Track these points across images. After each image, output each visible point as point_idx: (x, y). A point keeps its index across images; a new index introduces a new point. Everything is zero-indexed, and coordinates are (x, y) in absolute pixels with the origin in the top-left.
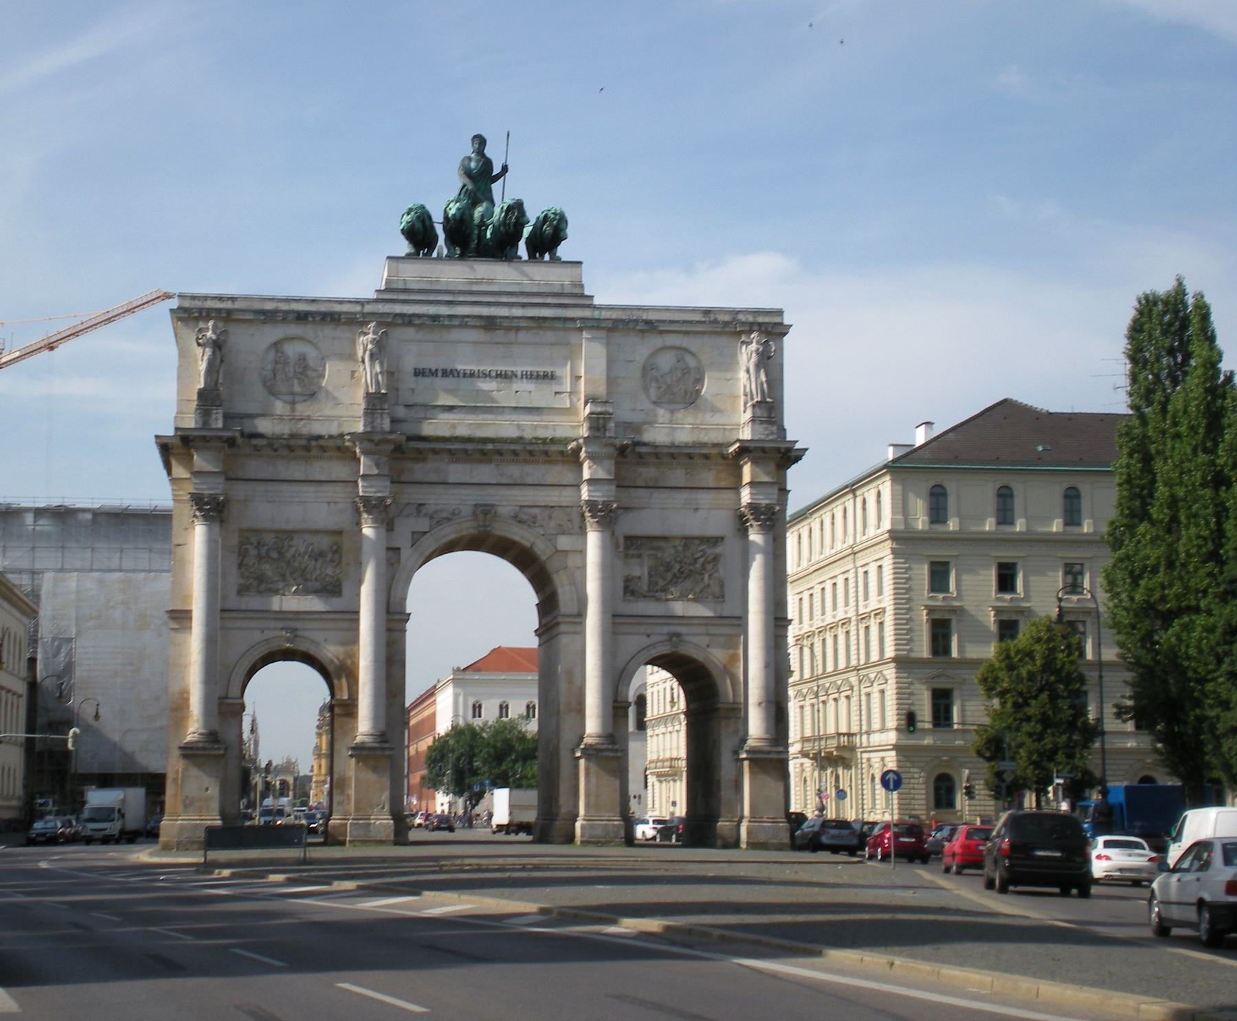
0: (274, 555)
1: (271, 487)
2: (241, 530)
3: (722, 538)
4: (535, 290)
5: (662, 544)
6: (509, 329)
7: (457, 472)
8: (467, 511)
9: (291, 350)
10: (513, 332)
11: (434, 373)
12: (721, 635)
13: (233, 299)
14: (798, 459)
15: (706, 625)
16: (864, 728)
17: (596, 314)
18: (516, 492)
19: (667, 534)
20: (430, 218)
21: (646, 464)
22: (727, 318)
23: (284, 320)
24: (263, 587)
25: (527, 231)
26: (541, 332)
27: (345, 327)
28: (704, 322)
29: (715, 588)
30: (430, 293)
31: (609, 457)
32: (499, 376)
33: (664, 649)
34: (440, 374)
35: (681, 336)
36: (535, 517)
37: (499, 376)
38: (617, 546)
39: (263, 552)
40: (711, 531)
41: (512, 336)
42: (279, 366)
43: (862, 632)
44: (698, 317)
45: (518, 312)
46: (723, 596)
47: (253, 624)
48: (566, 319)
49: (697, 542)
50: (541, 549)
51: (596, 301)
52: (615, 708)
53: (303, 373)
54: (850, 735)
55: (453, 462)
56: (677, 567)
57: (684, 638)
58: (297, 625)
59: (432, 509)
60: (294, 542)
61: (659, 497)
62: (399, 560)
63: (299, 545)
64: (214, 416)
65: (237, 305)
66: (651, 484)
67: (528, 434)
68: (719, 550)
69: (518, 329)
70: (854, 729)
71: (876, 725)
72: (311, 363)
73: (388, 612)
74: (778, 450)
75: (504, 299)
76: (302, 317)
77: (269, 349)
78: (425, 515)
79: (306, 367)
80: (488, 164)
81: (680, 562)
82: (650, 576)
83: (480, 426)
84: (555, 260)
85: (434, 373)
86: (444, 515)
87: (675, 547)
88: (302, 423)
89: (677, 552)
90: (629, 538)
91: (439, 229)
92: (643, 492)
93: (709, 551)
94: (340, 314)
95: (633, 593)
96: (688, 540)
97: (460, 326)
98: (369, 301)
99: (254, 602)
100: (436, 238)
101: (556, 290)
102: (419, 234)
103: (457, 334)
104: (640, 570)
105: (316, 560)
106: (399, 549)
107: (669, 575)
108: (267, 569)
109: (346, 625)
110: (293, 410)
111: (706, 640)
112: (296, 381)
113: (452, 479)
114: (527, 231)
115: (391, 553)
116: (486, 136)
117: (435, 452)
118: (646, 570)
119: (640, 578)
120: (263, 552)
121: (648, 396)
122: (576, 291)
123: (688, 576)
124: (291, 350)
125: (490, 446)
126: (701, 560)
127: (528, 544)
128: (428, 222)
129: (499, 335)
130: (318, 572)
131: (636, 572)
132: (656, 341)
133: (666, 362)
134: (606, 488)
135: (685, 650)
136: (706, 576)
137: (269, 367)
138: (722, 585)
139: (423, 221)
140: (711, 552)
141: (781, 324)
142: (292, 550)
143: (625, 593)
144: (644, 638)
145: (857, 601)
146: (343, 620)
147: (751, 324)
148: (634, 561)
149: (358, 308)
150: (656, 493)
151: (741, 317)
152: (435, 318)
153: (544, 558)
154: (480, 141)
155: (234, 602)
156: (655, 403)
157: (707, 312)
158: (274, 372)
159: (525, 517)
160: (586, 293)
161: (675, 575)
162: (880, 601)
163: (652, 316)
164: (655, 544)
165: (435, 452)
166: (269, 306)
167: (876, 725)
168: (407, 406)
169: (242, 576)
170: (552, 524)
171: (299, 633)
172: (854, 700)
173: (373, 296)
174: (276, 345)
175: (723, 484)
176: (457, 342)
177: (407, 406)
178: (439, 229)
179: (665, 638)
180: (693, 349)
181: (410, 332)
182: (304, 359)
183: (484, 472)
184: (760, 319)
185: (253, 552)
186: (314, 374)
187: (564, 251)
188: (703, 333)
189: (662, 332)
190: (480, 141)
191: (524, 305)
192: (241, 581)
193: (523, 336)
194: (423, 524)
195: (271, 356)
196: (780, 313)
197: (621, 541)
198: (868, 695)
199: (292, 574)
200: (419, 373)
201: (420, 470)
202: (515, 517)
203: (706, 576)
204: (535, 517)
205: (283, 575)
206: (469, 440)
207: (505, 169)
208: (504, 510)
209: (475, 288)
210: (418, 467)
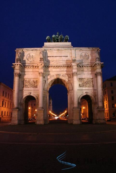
0: (28, 82)
5: (84, 79)
9: (31, 55)
18: (62, 72)
32: (60, 57)
37: (60, 57)
52: (78, 103)
53: (33, 57)
56: (87, 82)
68: (93, 80)
83: (57, 63)
107: (86, 84)
108: (27, 84)
110: (31, 62)
118: (82, 83)
131: (81, 83)
133: (83, 54)
152: (51, 49)
175: (93, 70)
180: (87, 53)
183: (58, 70)
189: (83, 50)
197: (78, 79)
208: (61, 75)
209: (56, 46)
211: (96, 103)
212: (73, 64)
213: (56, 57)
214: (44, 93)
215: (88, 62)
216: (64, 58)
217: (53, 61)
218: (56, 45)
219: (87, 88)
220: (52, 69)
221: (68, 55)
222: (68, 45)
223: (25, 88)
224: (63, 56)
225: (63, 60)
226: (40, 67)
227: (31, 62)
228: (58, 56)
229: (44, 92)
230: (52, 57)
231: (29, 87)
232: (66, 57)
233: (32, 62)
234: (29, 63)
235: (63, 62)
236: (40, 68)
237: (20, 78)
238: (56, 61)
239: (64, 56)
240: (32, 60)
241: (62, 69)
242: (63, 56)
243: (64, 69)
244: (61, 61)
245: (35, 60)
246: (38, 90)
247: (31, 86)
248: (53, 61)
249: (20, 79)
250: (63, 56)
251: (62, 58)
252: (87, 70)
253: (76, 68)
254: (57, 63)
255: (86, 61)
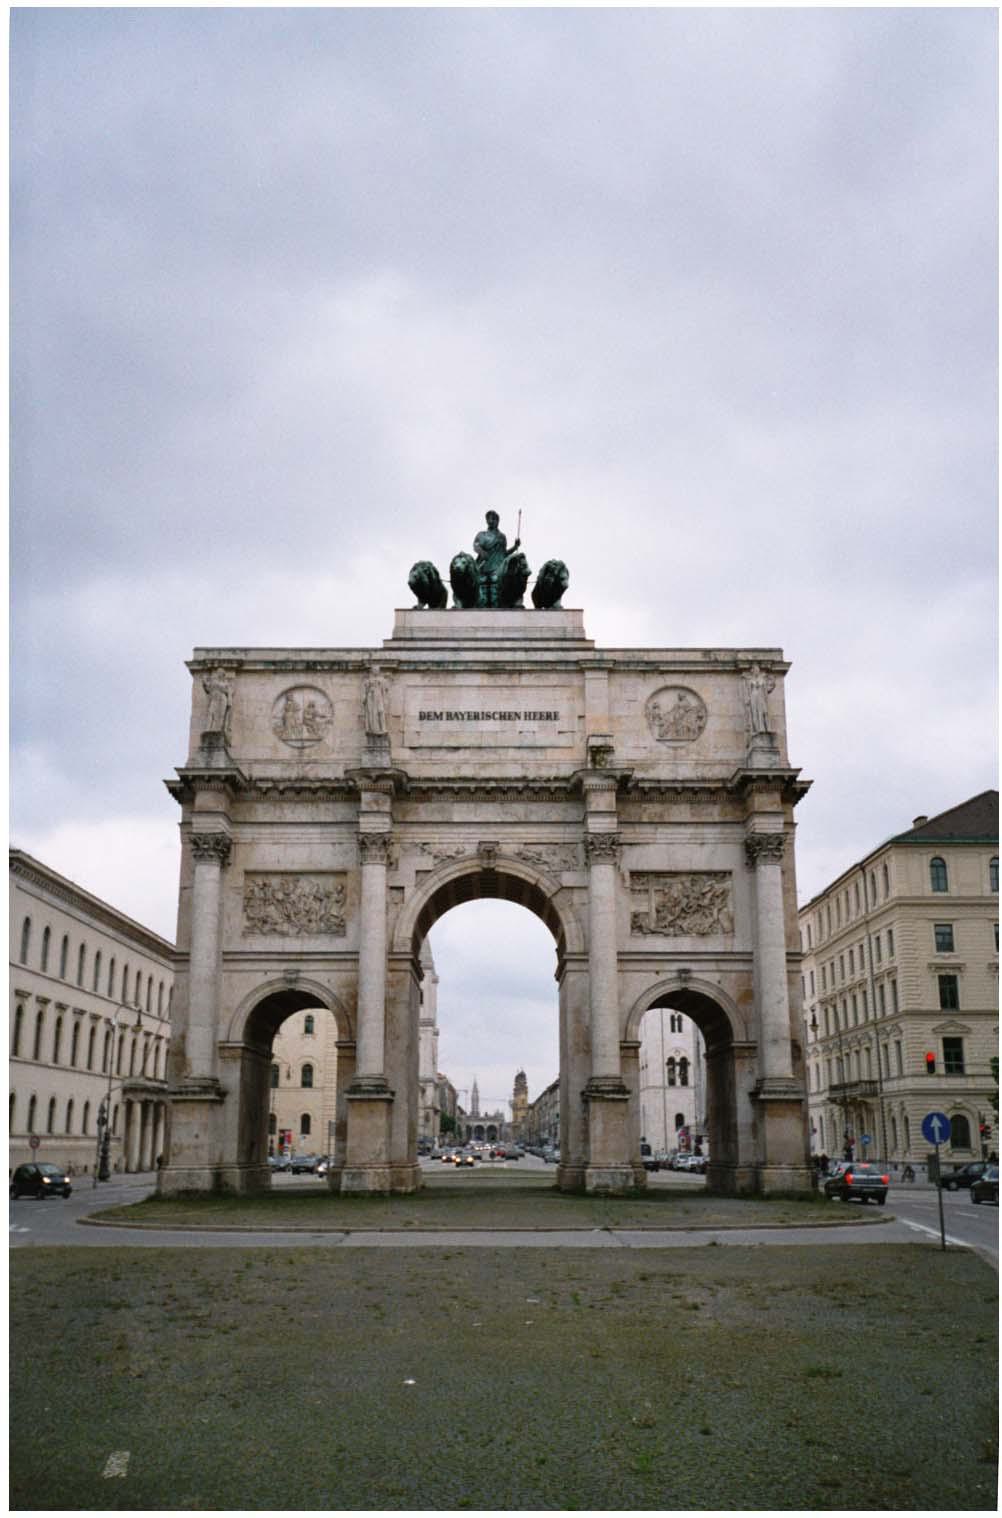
1: (275, 830)
2: (248, 873)
3: (730, 873)
4: (538, 635)
5: (668, 880)
6: (511, 672)
7: (461, 812)
8: (471, 850)
10: (516, 676)
11: (438, 717)
12: (731, 971)
13: (246, 650)
14: (804, 791)
15: (717, 961)
16: (884, 1076)
17: (598, 656)
18: (519, 829)
19: (673, 869)
20: (437, 573)
21: (651, 801)
22: (728, 657)
23: (294, 671)
24: (267, 928)
25: (531, 586)
26: (544, 675)
27: (352, 675)
28: (708, 662)
29: (726, 924)
30: (434, 640)
31: (609, 790)
32: (504, 717)
33: (674, 987)
34: (444, 716)
35: (682, 675)
36: (540, 854)
37: (504, 717)
38: (623, 880)
39: (269, 894)
40: (717, 866)
41: (515, 680)
42: (290, 713)
43: (877, 991)
44: (698, 657)
45: (520, 656)
46: (733, 931)
47: (257, 966)
48: (567, 662)
49: (705, 877)
50: (547, 886)
51: (597, 645)
54: (872, 1082)
55: (457, 802)
56: (685, 901)
57: (695, 975)
58: (302, 966)
59: (435, 849)
60: (300, 884)
61: (663, 833)
62: (403, 900)
63: (306, 886)
64: (215, 758)
65: (252, 656)
66: (656, 820)
67: (531, 775)
68: (727, 884)
69: (521, 672)
70: (876, 1077)
71: (894, 1073)
72: (320, 711)
73: (390, 952)
74: (781, 778)
75: (508, 644)
76: (311, 667)
77: (279, 698)
78: (430, 853)
79: (315, 715)
80: (502, 540)
81: (688, 897)
82: (658, 911)
83: (484, 765)
84: (561, 609)
85: (438, 717)
86: (449, 854)
87: (682, 883)
88: (308, 767)
89: (685, 888)
90: (636, 875)
91: (448, 586)
92: (648, 829)
93: (716, 886)
94: (347, 662)
95: (640, 928)
96: (694, 874)
97: (465, 671)
98: (376, 650)
99: (259, 944)
100: (444, 592)
101: (559, 635)
102: (426, 587)
103: (460, 679)
104: (648, 904)
105: (321, 900)
106: (402, 888)
108: (271, 910)
109: (349, 965)
110: (301, 755)
111: (717, 976)
112: (305, 728)
113: (456, 819)
114: (531, 586)
115: (394, 892)
116: (498, 512)
117: (441, 791)
118: (654, 905)
119: (647, 914)
120: (269, 894)
121: (652, 734)
122: (577, 636)
123: (697, 911)
124: (301, 699)
125: (493, 784)
126: (709, 895)
127: (533, 882)
128: (434, 576)
129: (502, 680)
130: (323, 912)
131: (643, 908)
132: (660, 681)
133: (668, 701)
134: (608, 820)
135: (693, 986)
136: (715, 911)
137: (280, 715)
138: (732, 920)
139: (430, 576)
140: (719, 887)
141: (781, 662)
142: (299, 891)
143: (633, 928)
144: (653, 975)
145: (872, 963)
146: (346, 960)
147: (751, 662)
148: (643, 896)
149: (366, 656)
150: (660, 829)
151: (741, 656)
152: (439, 663)
153: (549, 895)
154: (493, 518)
155: (237, 945)
156: (658, 740)
157: (707, 652)
158: (284, 719)
159: (530, 854)
160: (588, 637)
161: (683, 910)
162: (892, 962)
163: (653, 657)
164: (662, 880)
165: (441, 791)
166: (280, 657)
167: (894, 1073)
168: (411, 748)
169: (249, 918)
170: (556, 860)
171: (302, 975)
172: (874, 1051)
173: (381, 645)
174: (287, 694)
175: (729, 818)
176: (461, 686)
177: (411, 748)
178: (448, 586)
179: (675, 975)
180: (694, 688)
181: (416, 679)
182: (313, 706)
183: (489, 811)
184: (761, 657)
185: (258, 893)
186: (324, 720)
187: (567, 600)
188: (704, 672)
189: (663, 672)
190: (493, 518)
191: (526, 650)
192: (247, 924)
193: (525, 680)
194: (427, 863)
195: (282, 703)
196: (780, 651)
197: (627, 875)
198: (886, 1046)
199: (296, 914)
200: (423, 716)
201: (424, 811)
202: (519, 854)
203: (715, 911)
204: (540, 854)
205: (288, 916)
206: (473, 779)
207: (518, 543)
208: (508, 849)
210: (421, 806)
211: (753, 1050)
212: (591, 782)
213: (476, 717)
214: (390, 975)
215: (699, 754)
216: (533, 725)
217: (457, 749)
218: (476, 629)
219: (685, 944)
220: (447, 805)
221: (563, 709)
222: (564, 629)
223: (263, 938)
224: (529, 716)
225: (527, 743)
226: (365, 796)
227: (301, 755)
228: (490, 708)
229: (392, 970)
230: (450, 716)
231: (283, 934)
232: (549, 716)
233: (307, 751)
234: (287, 763)
235: (525, 754)
236: (368, 804)
237: (224, 864)
238: (480, 748)
239: (532, 709)
240: (306, 735)
241: (518, 810)
242: (522, 709)
243: (534, 807)
244: (511, 752)
245: (329, 740)
246: (353, 957)
247: (304, 921)
248: (457, 749)
249: (228, 877)
250: (529, 716)
251: (521, 724)
252: (693, 815)
253: (610, 805)
254: (484, 765)
255: (683, 752)
